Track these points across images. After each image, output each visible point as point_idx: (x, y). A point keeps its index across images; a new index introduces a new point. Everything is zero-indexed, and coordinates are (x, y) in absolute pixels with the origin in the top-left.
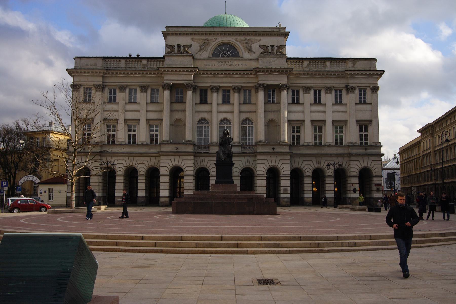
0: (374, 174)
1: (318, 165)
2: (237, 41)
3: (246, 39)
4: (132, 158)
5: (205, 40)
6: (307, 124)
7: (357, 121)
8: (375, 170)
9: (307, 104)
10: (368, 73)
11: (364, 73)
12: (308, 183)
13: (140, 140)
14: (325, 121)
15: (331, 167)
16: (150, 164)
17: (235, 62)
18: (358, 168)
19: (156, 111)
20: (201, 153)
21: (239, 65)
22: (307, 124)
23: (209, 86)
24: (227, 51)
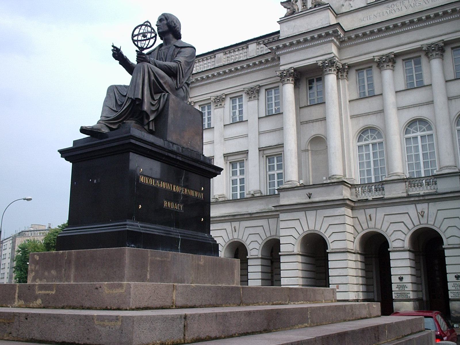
4: (236, 224)
13: (250, 190)
16: (268, 235)
20: (367, 200)
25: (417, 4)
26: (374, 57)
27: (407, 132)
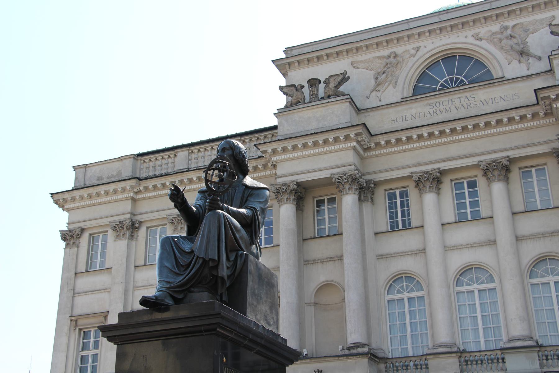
2: (481, 39)
3: (506, 28)
5: (389, 57)
21: (493, 100)
23: (409, 177)
25: (472, 105)
26: (412, 173)
27: (458, 283)
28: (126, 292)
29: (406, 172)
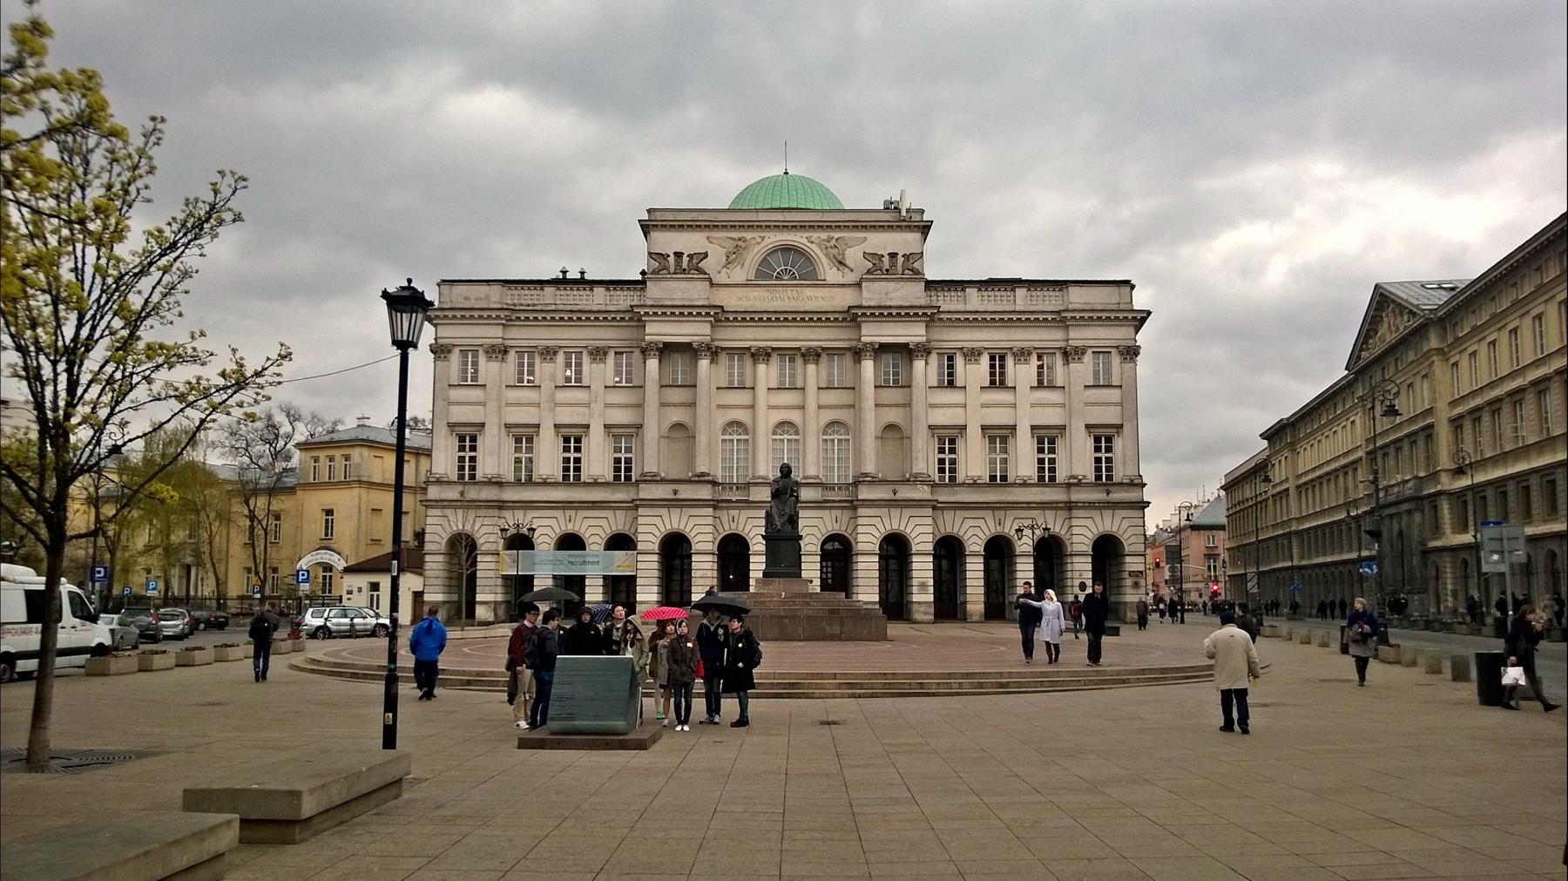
0: (1127, 549)
1: (999, 529)
6: (974, 433)
7: (1088, 427)
8: (1130, 543)
9: (973, 389)
10: (1112, 315)
11: (1104, 315)
12: (975, 570)
14: (1014, 428)
15: (1027, 532)
17: (809, 292)
18: (1090, 535)
19: (626, 406)
22: (974, 433)
24: (792, 265)
28: (500, 407)
29: (747, 344)
